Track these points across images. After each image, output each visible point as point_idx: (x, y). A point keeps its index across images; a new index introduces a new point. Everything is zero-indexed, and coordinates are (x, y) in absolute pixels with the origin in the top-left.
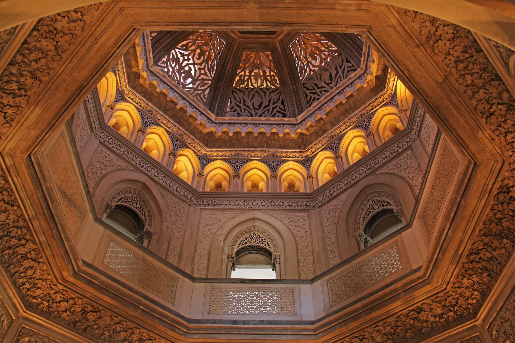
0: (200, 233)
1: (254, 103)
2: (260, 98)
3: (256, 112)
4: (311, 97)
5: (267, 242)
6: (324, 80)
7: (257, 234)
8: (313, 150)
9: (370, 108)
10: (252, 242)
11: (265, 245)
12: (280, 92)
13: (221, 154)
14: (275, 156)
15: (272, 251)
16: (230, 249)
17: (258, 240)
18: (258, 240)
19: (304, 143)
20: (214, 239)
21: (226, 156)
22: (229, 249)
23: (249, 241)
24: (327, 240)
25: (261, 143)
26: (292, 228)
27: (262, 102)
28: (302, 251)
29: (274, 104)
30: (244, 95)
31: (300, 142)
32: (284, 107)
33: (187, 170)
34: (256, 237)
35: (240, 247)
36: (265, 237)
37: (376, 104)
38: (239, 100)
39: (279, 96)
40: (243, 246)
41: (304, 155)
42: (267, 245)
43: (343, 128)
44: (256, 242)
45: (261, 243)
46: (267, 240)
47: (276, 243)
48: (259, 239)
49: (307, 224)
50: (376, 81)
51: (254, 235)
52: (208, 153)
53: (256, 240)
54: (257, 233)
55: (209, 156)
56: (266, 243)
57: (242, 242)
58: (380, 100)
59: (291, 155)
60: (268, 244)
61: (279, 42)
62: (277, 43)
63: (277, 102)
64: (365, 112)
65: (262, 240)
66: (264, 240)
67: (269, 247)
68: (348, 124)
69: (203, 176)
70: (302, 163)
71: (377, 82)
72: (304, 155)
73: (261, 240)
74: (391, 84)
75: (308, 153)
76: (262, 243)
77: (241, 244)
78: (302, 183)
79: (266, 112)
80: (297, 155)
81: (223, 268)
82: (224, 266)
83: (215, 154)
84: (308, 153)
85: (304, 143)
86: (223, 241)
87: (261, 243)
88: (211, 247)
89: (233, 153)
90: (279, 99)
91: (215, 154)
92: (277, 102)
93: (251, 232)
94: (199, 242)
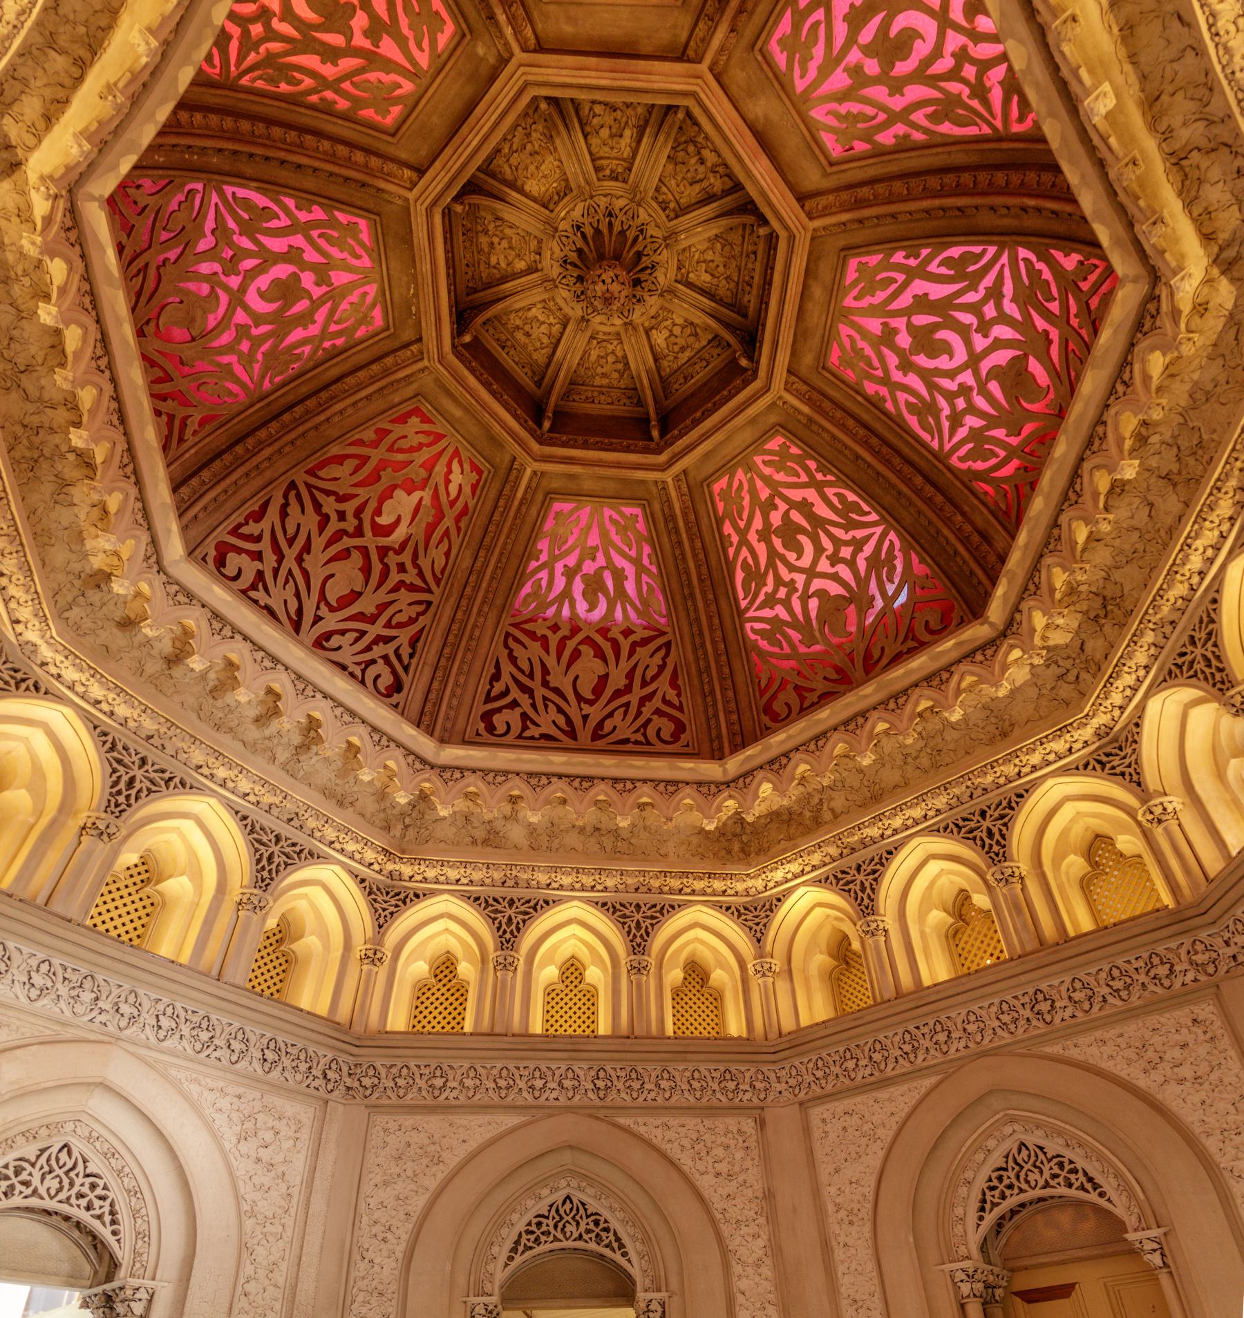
1: (332, 576)
2: (360, 577)
3: (319, 613)
4: (506, 692)
6: (577, 677)
9: (675, 883)
12: (429, 604)
17: (72, 1184)
18: (72, 1184)
27: (360, 594)
29: (388, 625)
30: (322, 528)
32: (411, 656)
36: (109, 1178)
37: (699, 885)
38: (291, 530)
39: (419, 614)
41: (390, 867)
43: (566, 881)
45: (83, 1202)
46: (116, 1193)
50: (729, 818)
58: (718, 885)
61: (535, 473)
62: (528, 472)
63: (400, 625)
64: (656, 883)
65: (93, 1187)
66: (99, 1191)
68: (588, 881)
70: (370, 891)
71: (730, 822)
72: (390, 867)
73: (86, 1190)
74: (779, 875)
75: (407, 870)
76: (89, 1208)
79: (351, 636)
84: (407, 870)
85: (407, 821)
87: (83, 1202)
90: (412, 621)
92: (400, 625)
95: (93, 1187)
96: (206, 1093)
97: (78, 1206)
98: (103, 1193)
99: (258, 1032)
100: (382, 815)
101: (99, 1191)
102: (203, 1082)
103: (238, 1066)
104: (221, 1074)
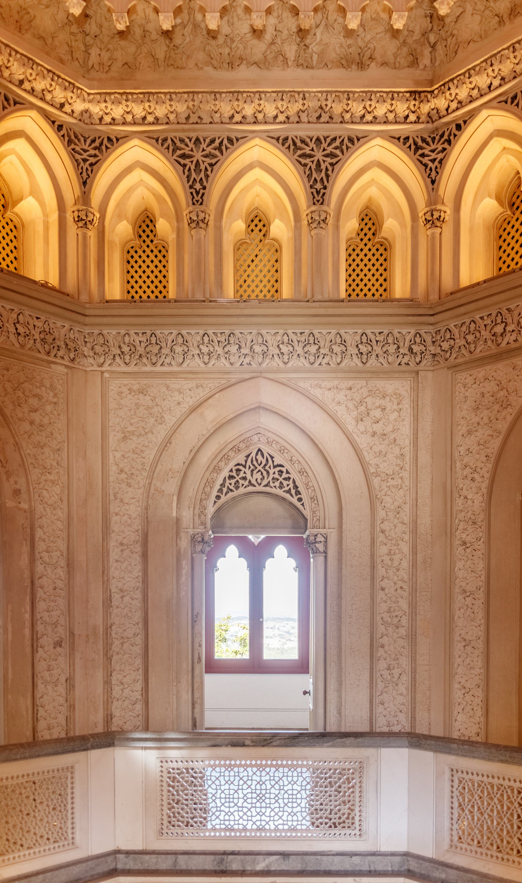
0: (113, 469)
5: (294, 482)
7: (266, 454)
8: (463, 93)
10: (254, 482)
11: (289, 491)
13: (138, 111)
14: (325, 118)
15: (307, 513)
16: (197, 512)
19: (432, 38)
20: (152, 491)
21: (157, 121)
22: (194, 514)
23: (244, 478)
24: (460, 501)
25: (279, 41)
26: (363, 442)
28: (386, 526)
31: (417, 36)
33: (35, 192)
34: (264, 462)
35: (223, 499)
36: (287, 466)
40: (230, 494)
41: (425, 108)
42: (293, 492)
44: (265, 482)
45: (277, 484)
47: (318, 491)
48: (271, 471)
49: (406, 428)
51: (259, 457)
52: (96, 110)
53: (265, 473)
54: (266, 449)
55: (101, 119)
56: (291, 486)
57: (228, 481)
59: (381, 110)
60: (296, 487)
65: (281, 472)
66: (285, 475)
67: (300, 500)
69: (91, 222)
72: (425, 108)
73: (276, 476)
76: (281, 486)
77: (225, 490)
78: (403, 225)
80: (401, 108)
81: (183, 579)
82: (184, 572)
83: (117, 112)
84: (441, 103)
85: (432, 38)
86: (175, 498)
87: (277, 484)
88: (146, 521)
89: (181, 108)
91: (117, 112)
93: (251, 448)
94: (112, 497)
95: (281, 472)
96: (327, 393)
97: (275, 487)
98: (287, 476)
99: (351, 331)
100: (405, 50)
101: (285, 475)
102: (323, 385)
103: (343, 365)
104: (333, 375)
